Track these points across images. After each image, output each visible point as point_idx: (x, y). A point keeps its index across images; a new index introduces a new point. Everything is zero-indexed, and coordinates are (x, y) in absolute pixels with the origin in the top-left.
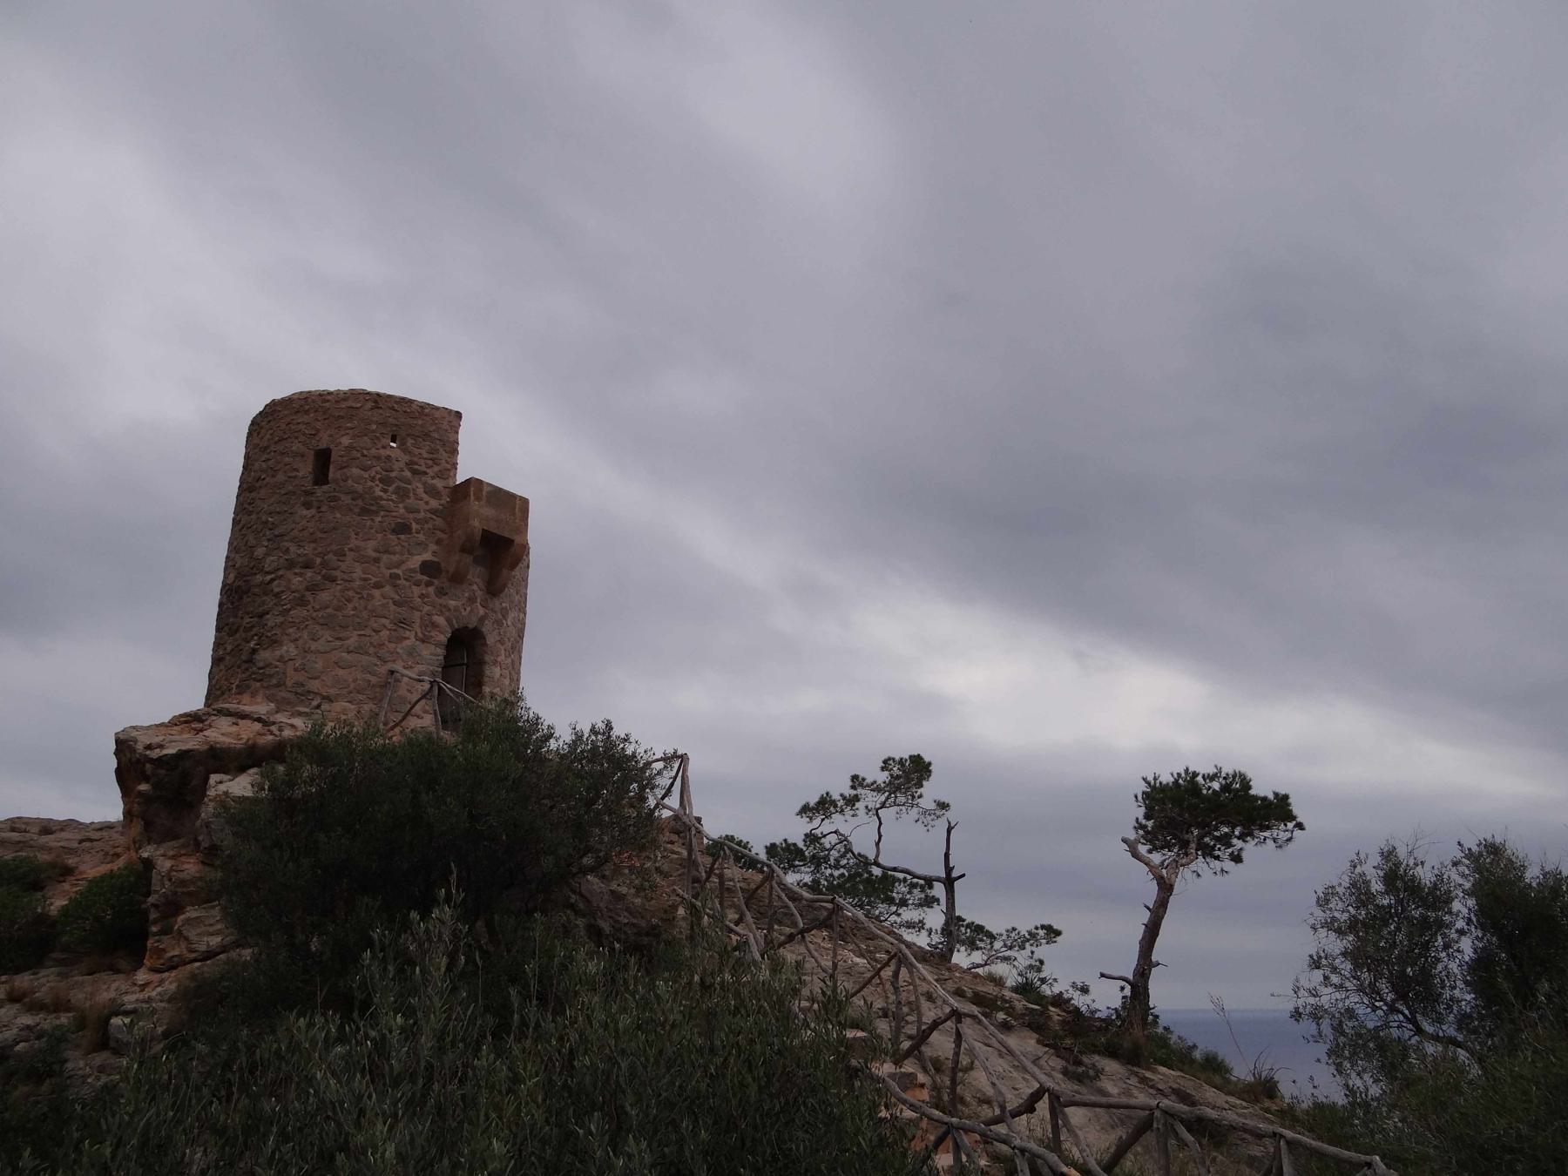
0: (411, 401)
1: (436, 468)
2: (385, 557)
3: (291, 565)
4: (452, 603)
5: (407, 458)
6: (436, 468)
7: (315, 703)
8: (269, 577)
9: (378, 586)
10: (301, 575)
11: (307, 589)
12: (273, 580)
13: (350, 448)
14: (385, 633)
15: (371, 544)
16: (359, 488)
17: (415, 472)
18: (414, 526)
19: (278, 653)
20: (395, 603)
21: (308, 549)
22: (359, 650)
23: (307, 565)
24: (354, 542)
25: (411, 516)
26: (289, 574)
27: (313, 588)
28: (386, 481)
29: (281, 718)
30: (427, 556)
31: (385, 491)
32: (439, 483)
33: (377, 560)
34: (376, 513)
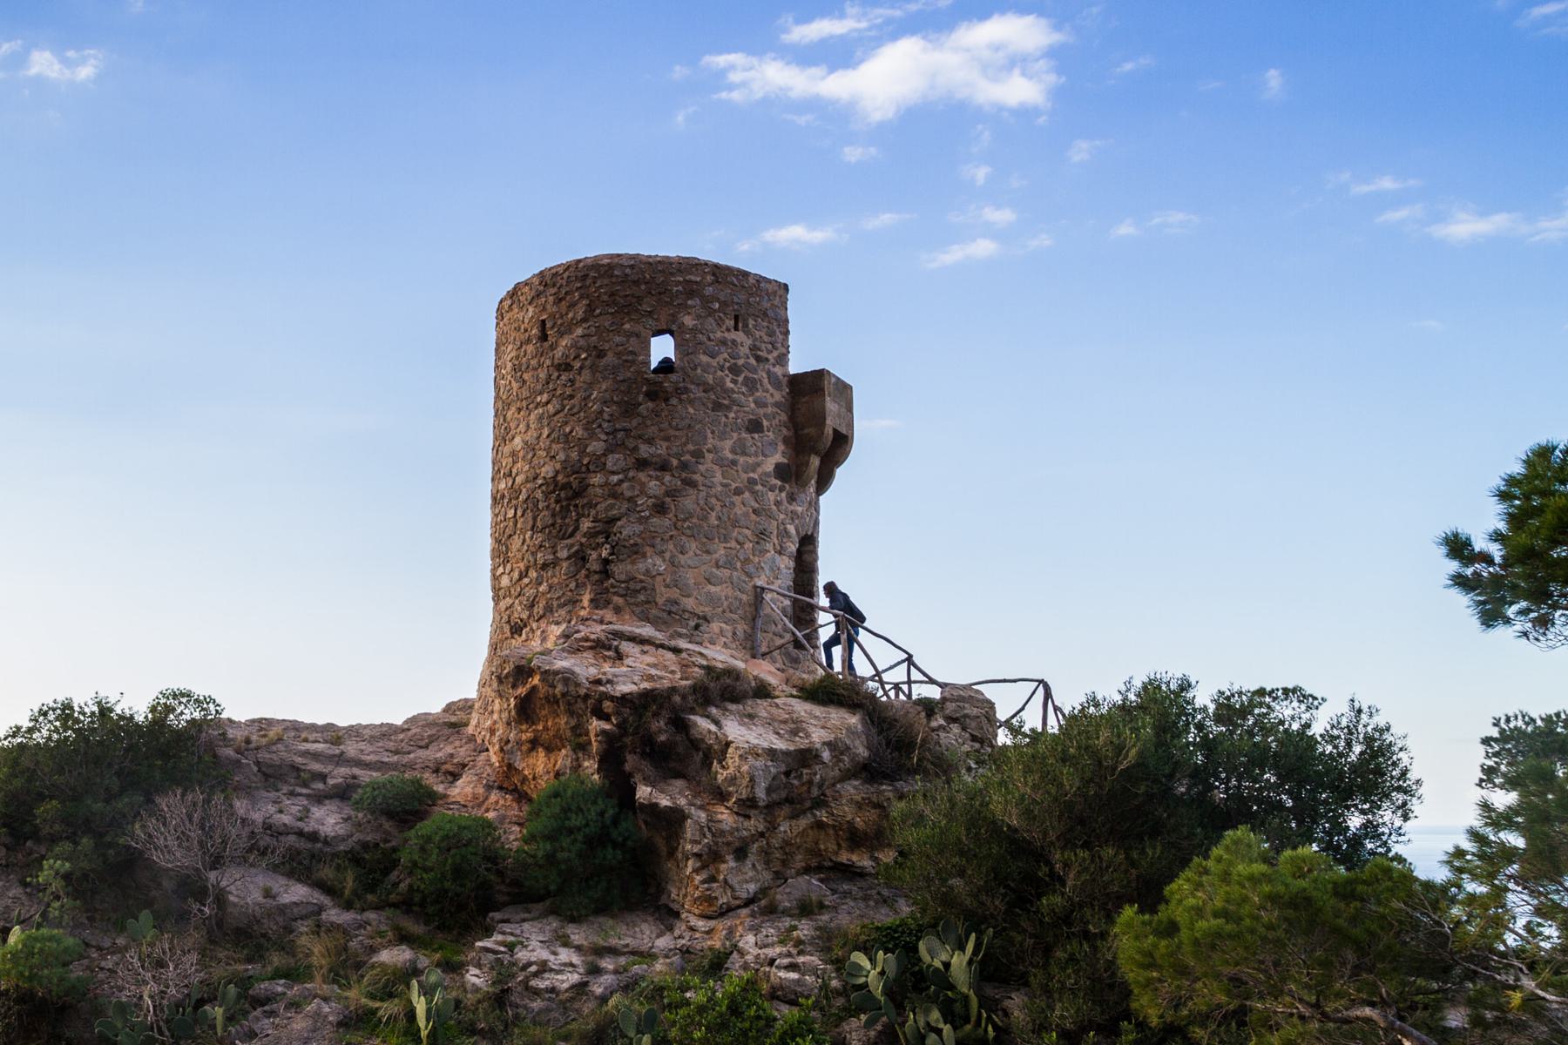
0: (746, 274)
1: (775, 354)
2: (742, 460)
3: (642, 464)
4: (800, 509)
5: (750, 342)
6: (775, 354)
7: (692, 624)
8: (615, 478)
9: (738, 492)
10: (657, 478)
11: (668, 494)
12: (621, 481)
13: (694, 330)
14: (749, 545)
15: (728, 444)
16: (710, 379)
17: (758, 359)
18: (765, 423)
19: (641, 566)
20: (754, 511)
21: (661, 449)
22: (729, 565)
23: (664, 467)
24: (711, 441)
25: (761, 411)
26: (642, 476)
27: (672, 493)
28: (735, 370)
31: (735, 382)
32: (778, 370)
33: (734, 463)
34: (728, 408)
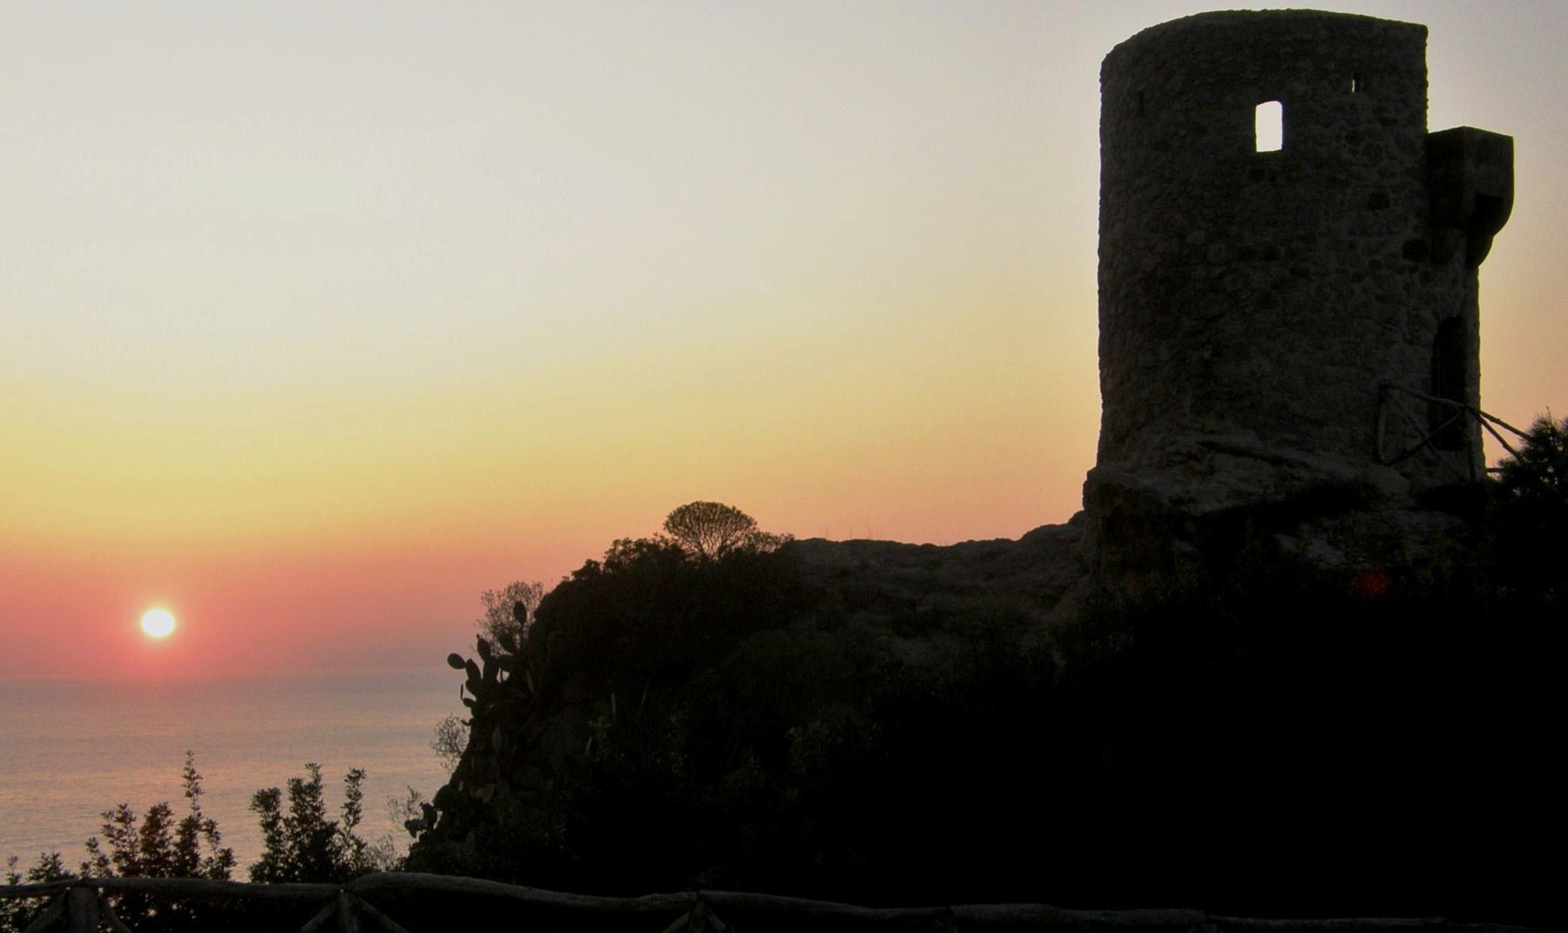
9: (1358, 278)
17: (1385, 122)
18: (1392, 196)
20: (1378, 299)
23: (1271, 256)
28: (1353, 138)
29: (1291, 454)
30: (1409, 234)
31: (1355, 153)
33: (1352, 246)
